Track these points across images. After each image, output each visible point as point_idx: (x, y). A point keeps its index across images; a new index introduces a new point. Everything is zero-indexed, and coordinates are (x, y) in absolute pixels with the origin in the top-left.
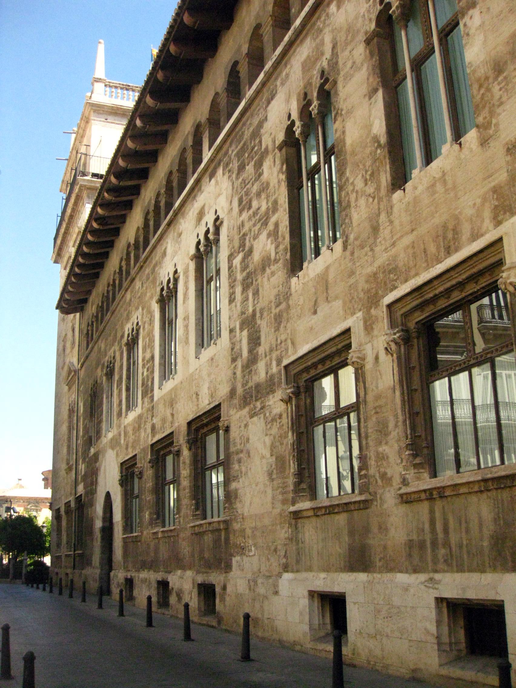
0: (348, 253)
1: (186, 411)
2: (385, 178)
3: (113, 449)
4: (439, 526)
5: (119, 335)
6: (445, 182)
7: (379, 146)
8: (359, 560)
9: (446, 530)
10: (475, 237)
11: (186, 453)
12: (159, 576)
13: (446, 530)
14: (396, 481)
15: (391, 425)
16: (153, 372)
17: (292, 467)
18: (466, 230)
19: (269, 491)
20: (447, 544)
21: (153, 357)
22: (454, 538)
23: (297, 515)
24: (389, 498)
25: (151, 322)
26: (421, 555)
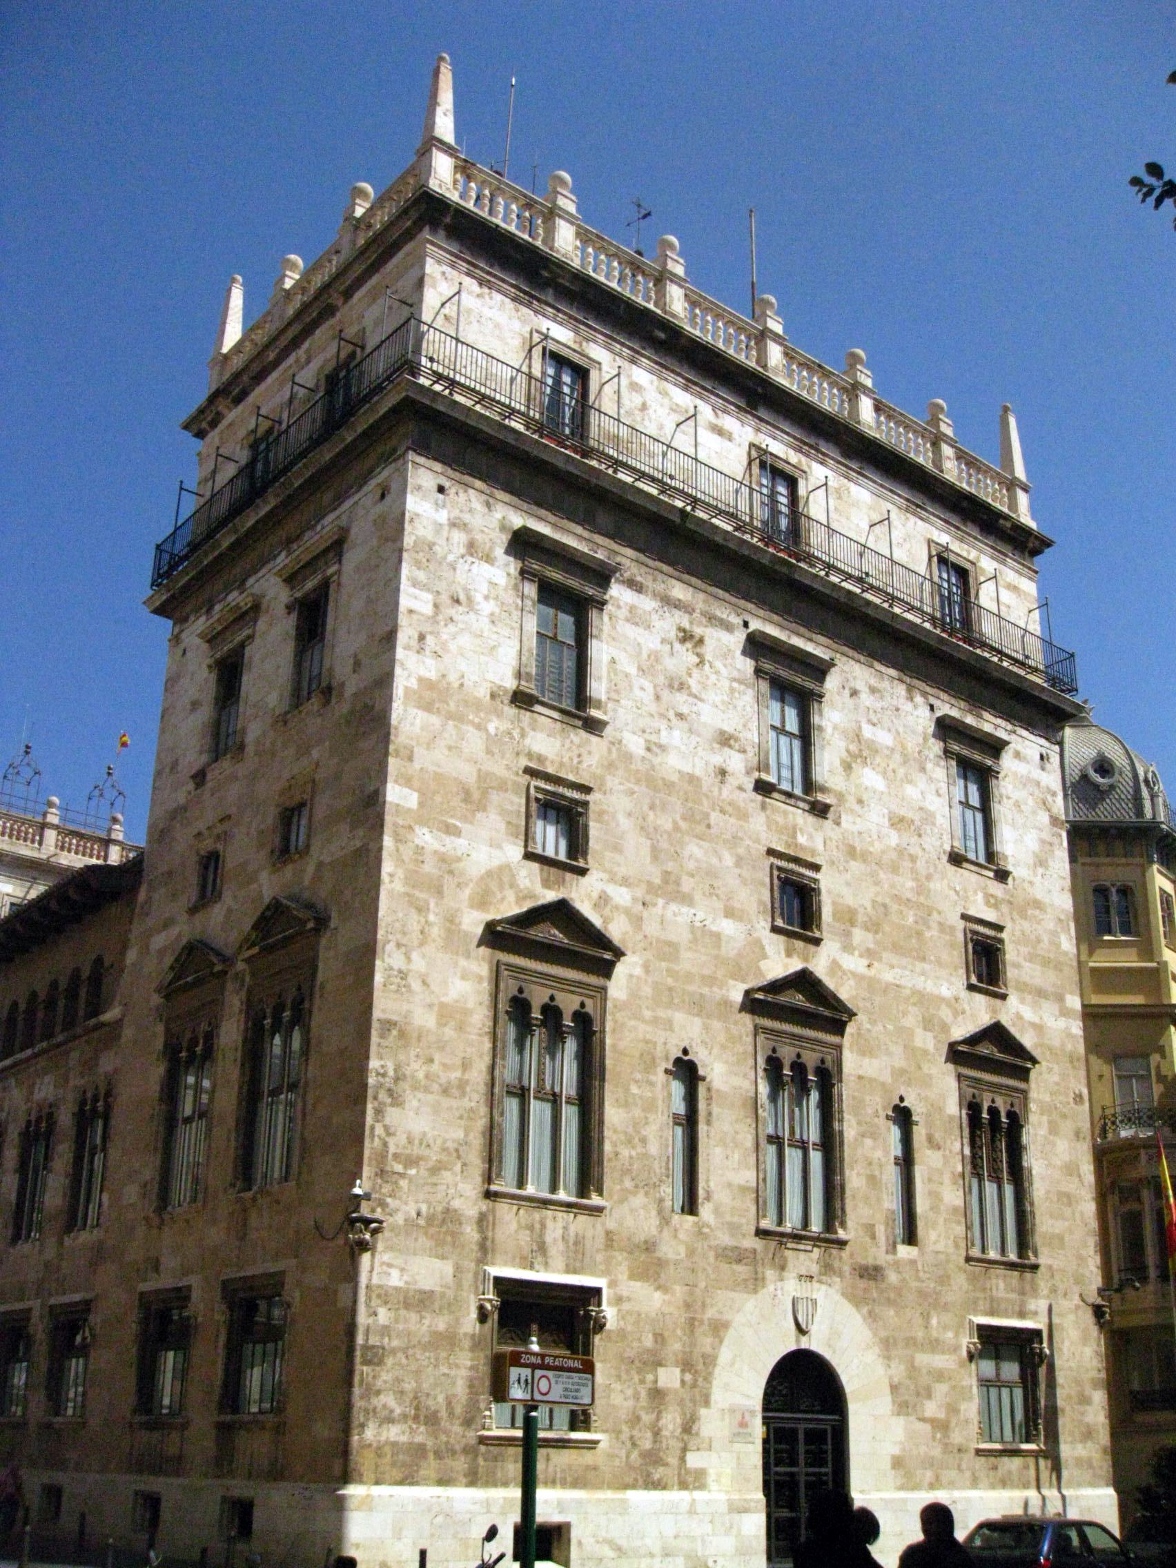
2: (10, 1232)
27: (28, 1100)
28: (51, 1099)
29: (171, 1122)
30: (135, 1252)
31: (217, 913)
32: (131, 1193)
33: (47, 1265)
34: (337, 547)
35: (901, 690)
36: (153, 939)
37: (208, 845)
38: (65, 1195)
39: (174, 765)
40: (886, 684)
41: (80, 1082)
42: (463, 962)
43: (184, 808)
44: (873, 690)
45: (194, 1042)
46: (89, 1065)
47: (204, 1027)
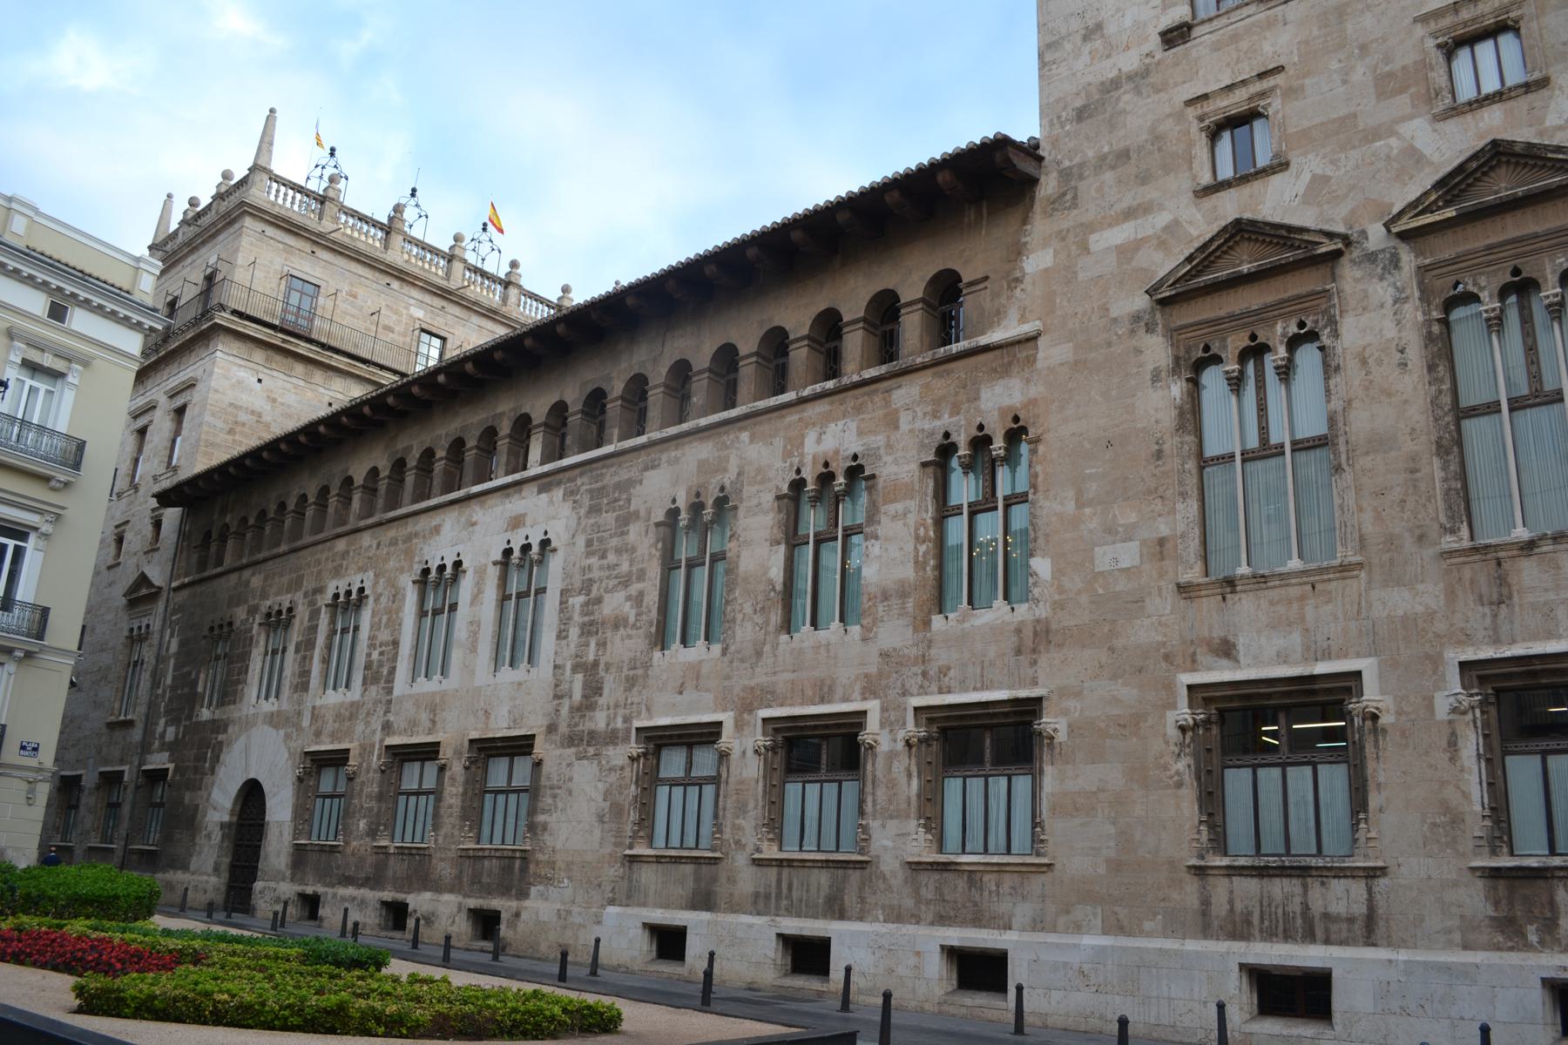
0: (726, 659)
3: (276, 727)
4: (784, 886)
5: (309, 584)
6: (828, 651)
7: (774, 589)
8: (703, 900)
9: (790, 888)
10: (846, 700)
11: (457, 769)
12: (388, 895)
13: (790, 888)
14: (750, 848)
15: (751, 806)
16: (395, 658)
17: (634, 816)
18: (839, 692)
19: (597, 833)
20: (789, 897)
21: (396, 643)
22: (795, 894)
23: (633, 859)
24: (741, 860)
25: (397, 596)
26: (761, 903)
27: (787, 454)
28: (855, 447)
33: (885, 655)
36: (1093, 238)
38: (919, 565)
39: (1093, 32)
43: (1144, 73)
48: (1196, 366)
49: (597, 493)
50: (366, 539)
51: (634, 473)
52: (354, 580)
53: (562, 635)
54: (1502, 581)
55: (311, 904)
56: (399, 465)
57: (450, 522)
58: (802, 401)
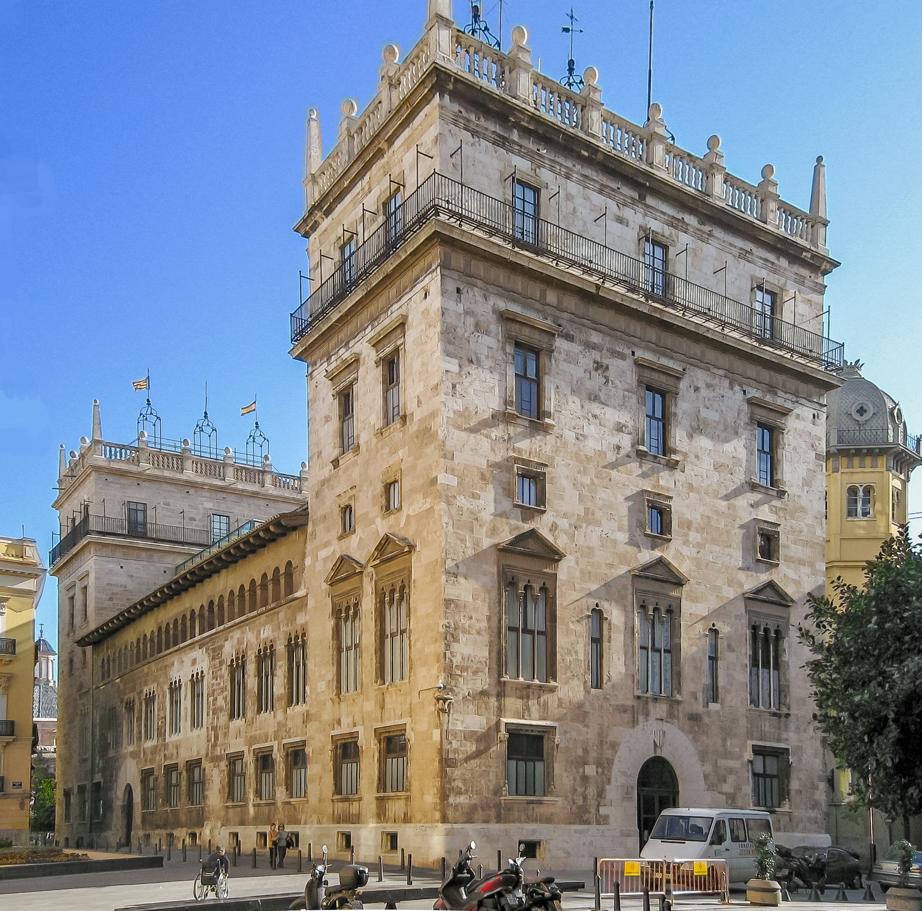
1: (184, 756)
3: (133, 758)
5: (138, 689)
8: (242, 823)
11: (184, 773)
17: (227, 790)
29: (339, 650)
30: (327, 715)
31: (354, 540)
32: (322, 686)
34: (402, 325)
35: (726, 383)
37: (344, 502)
40: (717, 381)
41: (286, 629)
42: (485, 566)
44: (709, 386)
45: (348, 608)
46: (292, 620)
47: (353, 600)
48: (337, 613)
49: (214, 650)
50: (153, 667)
51: (220, 644)
52: (153, 687)
53: (208, 715)
54: (384, 700)
55: (148, 837)
56: (160, 629)
57: (175, 659)
58: (259, 615)
